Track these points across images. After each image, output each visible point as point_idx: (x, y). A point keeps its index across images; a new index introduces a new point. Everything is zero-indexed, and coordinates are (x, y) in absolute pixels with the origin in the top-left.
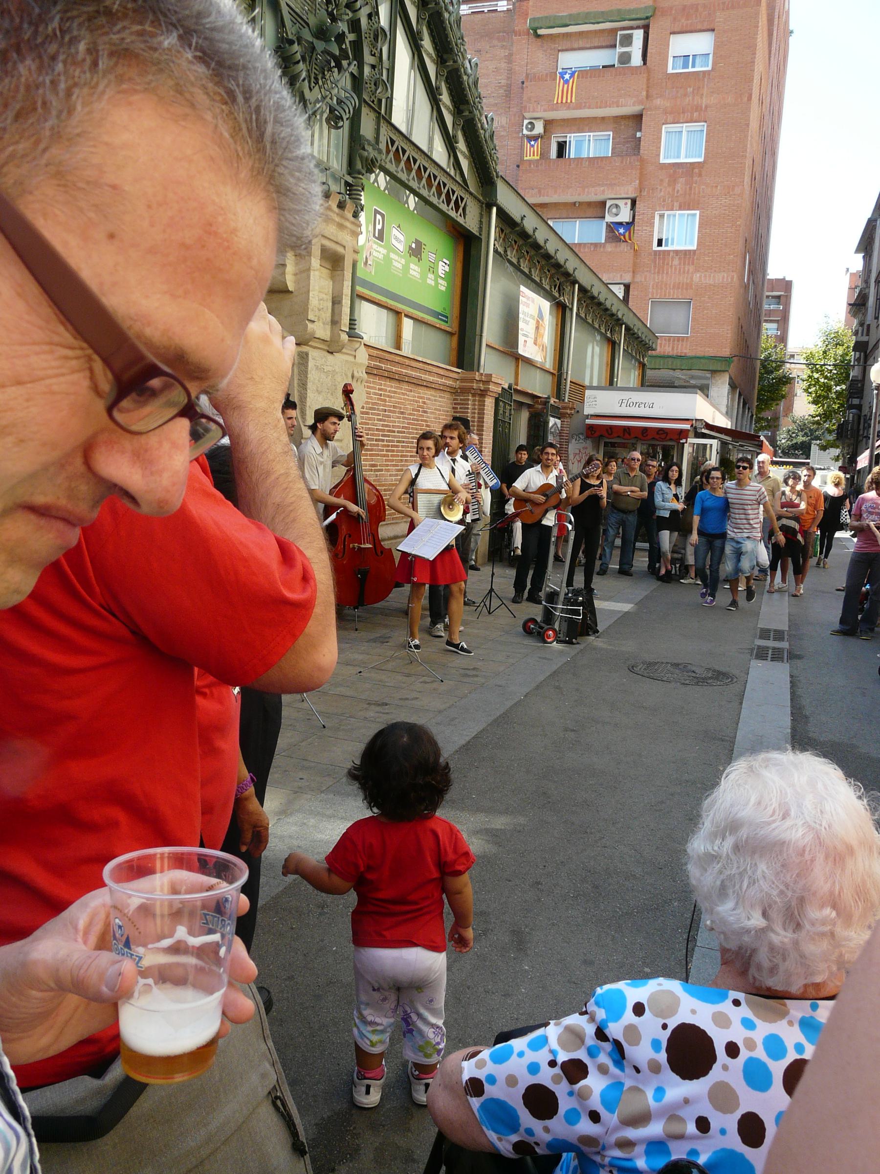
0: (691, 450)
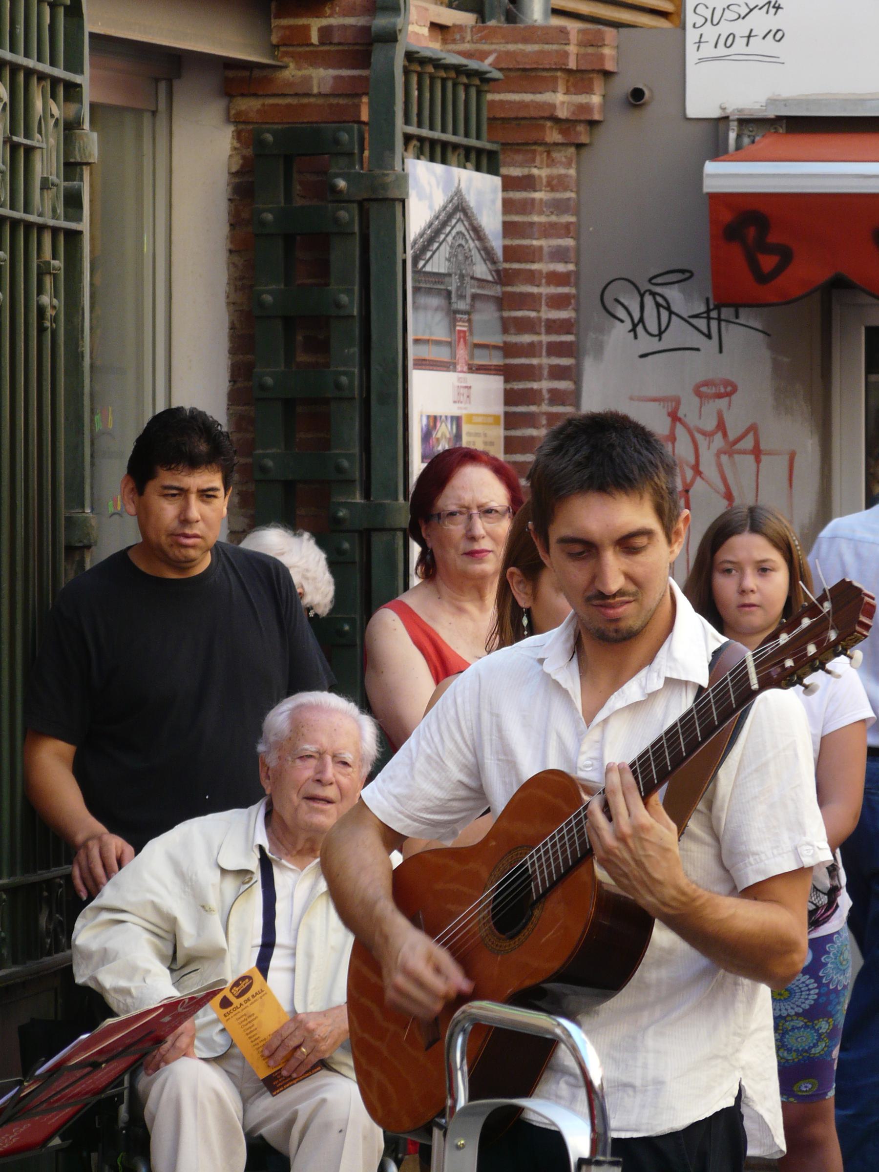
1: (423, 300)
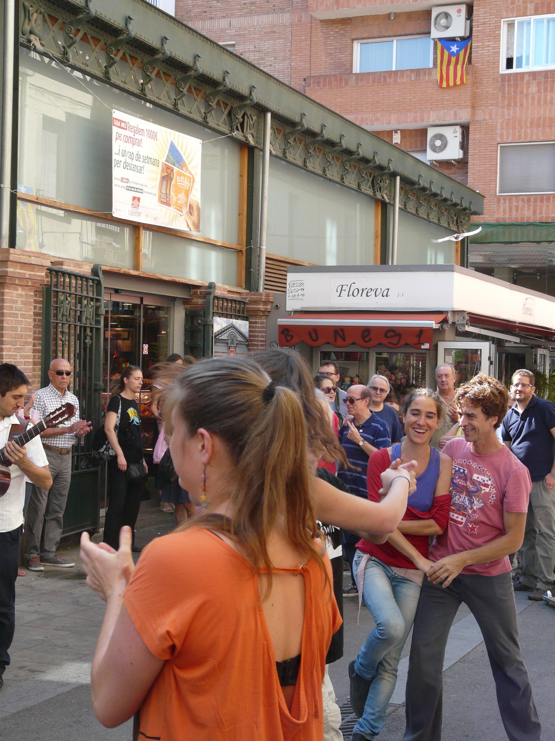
0: (450, 359)
1: (216, 344)
